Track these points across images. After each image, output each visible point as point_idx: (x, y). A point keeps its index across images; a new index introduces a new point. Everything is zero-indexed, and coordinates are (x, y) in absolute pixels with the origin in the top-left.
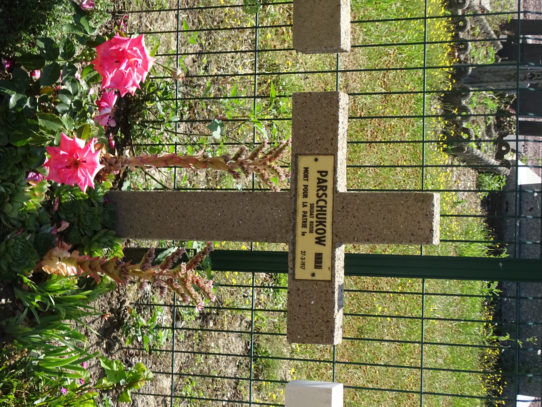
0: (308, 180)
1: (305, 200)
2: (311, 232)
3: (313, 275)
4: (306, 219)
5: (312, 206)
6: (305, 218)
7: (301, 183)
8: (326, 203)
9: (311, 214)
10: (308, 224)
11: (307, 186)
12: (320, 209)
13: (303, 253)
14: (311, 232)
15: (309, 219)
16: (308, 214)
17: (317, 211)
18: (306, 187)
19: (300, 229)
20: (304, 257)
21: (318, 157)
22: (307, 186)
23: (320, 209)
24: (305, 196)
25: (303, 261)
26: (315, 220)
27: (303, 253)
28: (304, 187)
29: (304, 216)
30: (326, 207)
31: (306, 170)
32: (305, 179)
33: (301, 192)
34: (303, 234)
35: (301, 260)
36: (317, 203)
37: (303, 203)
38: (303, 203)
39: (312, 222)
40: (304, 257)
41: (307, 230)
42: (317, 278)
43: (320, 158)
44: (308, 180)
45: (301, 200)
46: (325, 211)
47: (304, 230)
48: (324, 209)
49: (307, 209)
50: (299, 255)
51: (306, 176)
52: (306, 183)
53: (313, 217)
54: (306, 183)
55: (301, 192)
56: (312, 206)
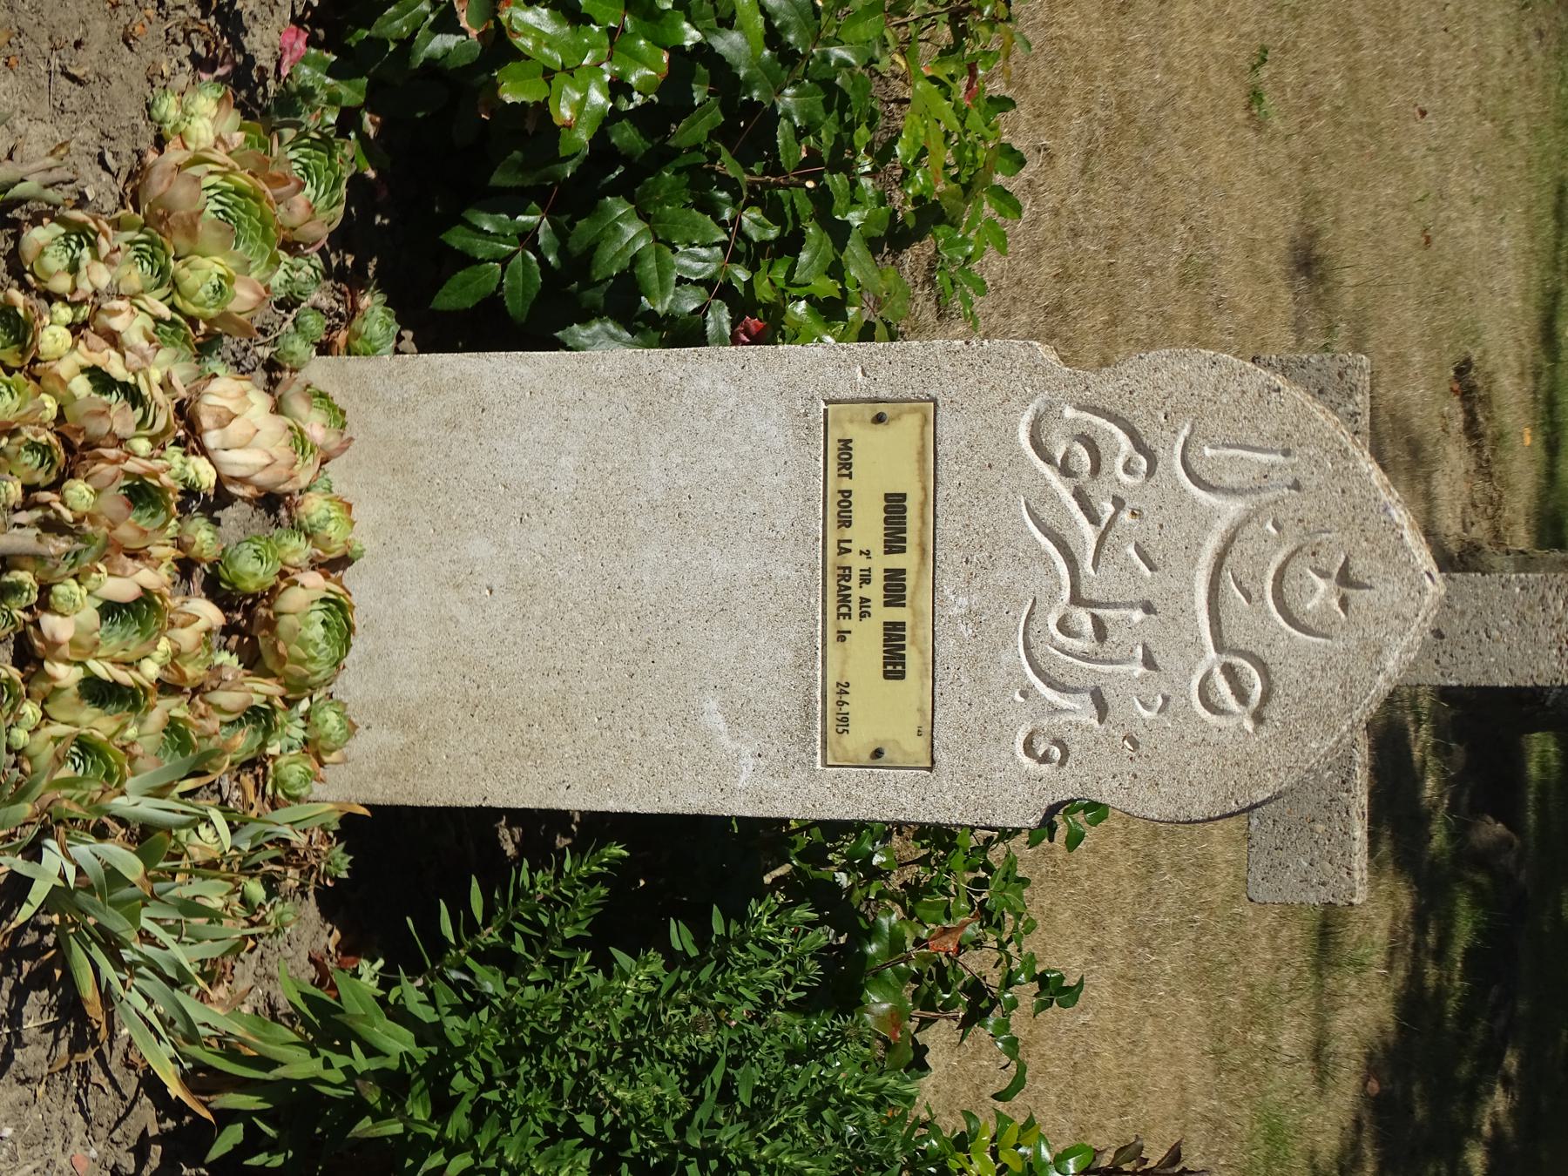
0: (850, 476)
10: (855, 605)
11: (850, 492)
13: (843, 688)
20: (845, 698)
21: (881, 408)
22: (850, 492)
24: (845, 522)
25: (845, 709)
31: (846, 445)
32: (845, 472)
40: (845, 698)
44: (850, 476)
51: (846, 465)
52: (846, 484)
54: (846, 484)
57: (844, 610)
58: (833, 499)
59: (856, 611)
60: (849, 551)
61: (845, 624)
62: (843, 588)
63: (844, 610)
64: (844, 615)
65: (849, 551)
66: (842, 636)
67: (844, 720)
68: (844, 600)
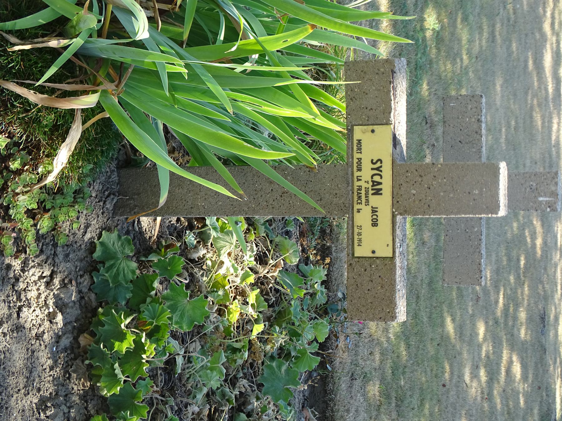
0: (361, 153)
1: (359, 174)
7: (356, 156)
18: (360, 159)
24: (359, 170)
25: (360, 237)
28: (357, 161)
31: (359, 141)
32: (359, 151)
33: (355, 165)
35: (357, 237)
37: (357, 177)
38: (357, 177)
42: (377, 255)
44: (361, 153)
45: (356, 174)
51: (359, 149)
52: (359, 156)
54: (359, 156)
55: (355, 165)
57: (359, 201)
58: (355, 161)
60: (361, 180)
61: (359, 206)
62: (358, 193)
63: (359, 201)
64: (359, 203)
65: (361, 180)
66: (359, 211)
67: (360, 240)
68: (359, 198)
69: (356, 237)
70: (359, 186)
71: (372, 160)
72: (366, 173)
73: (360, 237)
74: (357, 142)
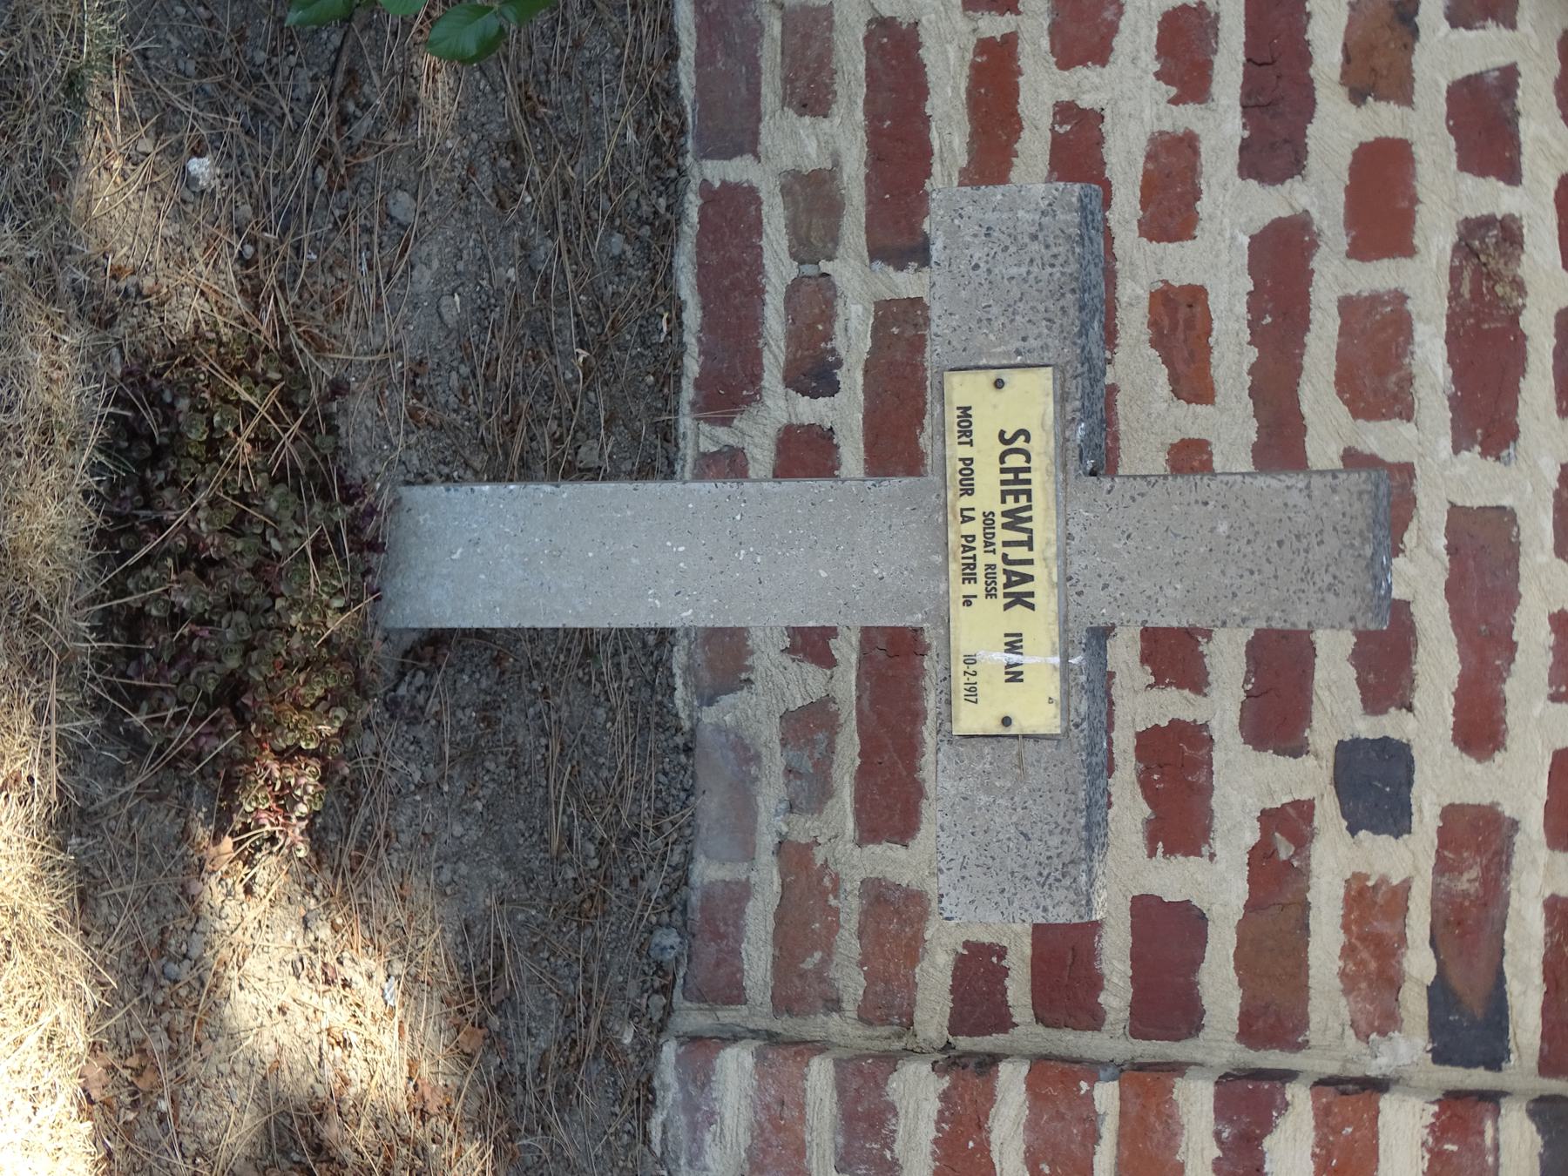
0: (971, 443)
1: (966, 501)
2: (990, 594)
3: (1006, 721)
4: (974, 557)
5: (988, 518)
6: (970, 554)
7: (957, 451)
8: (1028, 460)
9: (987, 544)
10: (980, 571)
12: (1010, 476)
14: (990, 594)
15: (983, 559)
16: (979, 543)
17: (1003, 482)
18: (968, 462)
19: (959, 589)
20: (972, 668)
23: (1010, 476)
24: (968, 490)
25: (973, 679)
26: (996, 559)
27: (970, 660)
28: (961, 465)
29: (966, 549)
30: (1028, 470)
31: (965, 412)
32: (964, 439)
33: (954, 478)
34: (968, 601)
35: (964, 679)
36: (1002, 461)
39: (989, 566)
41: (979, 588)
43: (1005, 375)
44: (971, 443)
46: (1028, 482)
47: (969, 589)
48: (1022, 476)
49: (975, 528)
50: (958, 668)
51: (966, 432)
52: (965, 451)
53: (994, 551)
54: (965, 451)
56: (988, 518)
59: (981, 578)
60: (973, 519)
65: (973, 519)
67: (972, 690)
69: (960, 682)
70: (966, 537)
71: (1002, 433)
72: (988, 495)
73: (973, 679)
74: (958, 413)
